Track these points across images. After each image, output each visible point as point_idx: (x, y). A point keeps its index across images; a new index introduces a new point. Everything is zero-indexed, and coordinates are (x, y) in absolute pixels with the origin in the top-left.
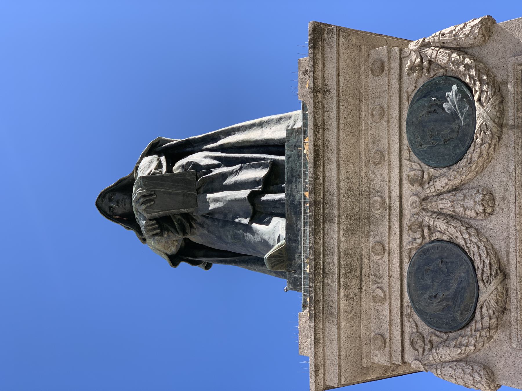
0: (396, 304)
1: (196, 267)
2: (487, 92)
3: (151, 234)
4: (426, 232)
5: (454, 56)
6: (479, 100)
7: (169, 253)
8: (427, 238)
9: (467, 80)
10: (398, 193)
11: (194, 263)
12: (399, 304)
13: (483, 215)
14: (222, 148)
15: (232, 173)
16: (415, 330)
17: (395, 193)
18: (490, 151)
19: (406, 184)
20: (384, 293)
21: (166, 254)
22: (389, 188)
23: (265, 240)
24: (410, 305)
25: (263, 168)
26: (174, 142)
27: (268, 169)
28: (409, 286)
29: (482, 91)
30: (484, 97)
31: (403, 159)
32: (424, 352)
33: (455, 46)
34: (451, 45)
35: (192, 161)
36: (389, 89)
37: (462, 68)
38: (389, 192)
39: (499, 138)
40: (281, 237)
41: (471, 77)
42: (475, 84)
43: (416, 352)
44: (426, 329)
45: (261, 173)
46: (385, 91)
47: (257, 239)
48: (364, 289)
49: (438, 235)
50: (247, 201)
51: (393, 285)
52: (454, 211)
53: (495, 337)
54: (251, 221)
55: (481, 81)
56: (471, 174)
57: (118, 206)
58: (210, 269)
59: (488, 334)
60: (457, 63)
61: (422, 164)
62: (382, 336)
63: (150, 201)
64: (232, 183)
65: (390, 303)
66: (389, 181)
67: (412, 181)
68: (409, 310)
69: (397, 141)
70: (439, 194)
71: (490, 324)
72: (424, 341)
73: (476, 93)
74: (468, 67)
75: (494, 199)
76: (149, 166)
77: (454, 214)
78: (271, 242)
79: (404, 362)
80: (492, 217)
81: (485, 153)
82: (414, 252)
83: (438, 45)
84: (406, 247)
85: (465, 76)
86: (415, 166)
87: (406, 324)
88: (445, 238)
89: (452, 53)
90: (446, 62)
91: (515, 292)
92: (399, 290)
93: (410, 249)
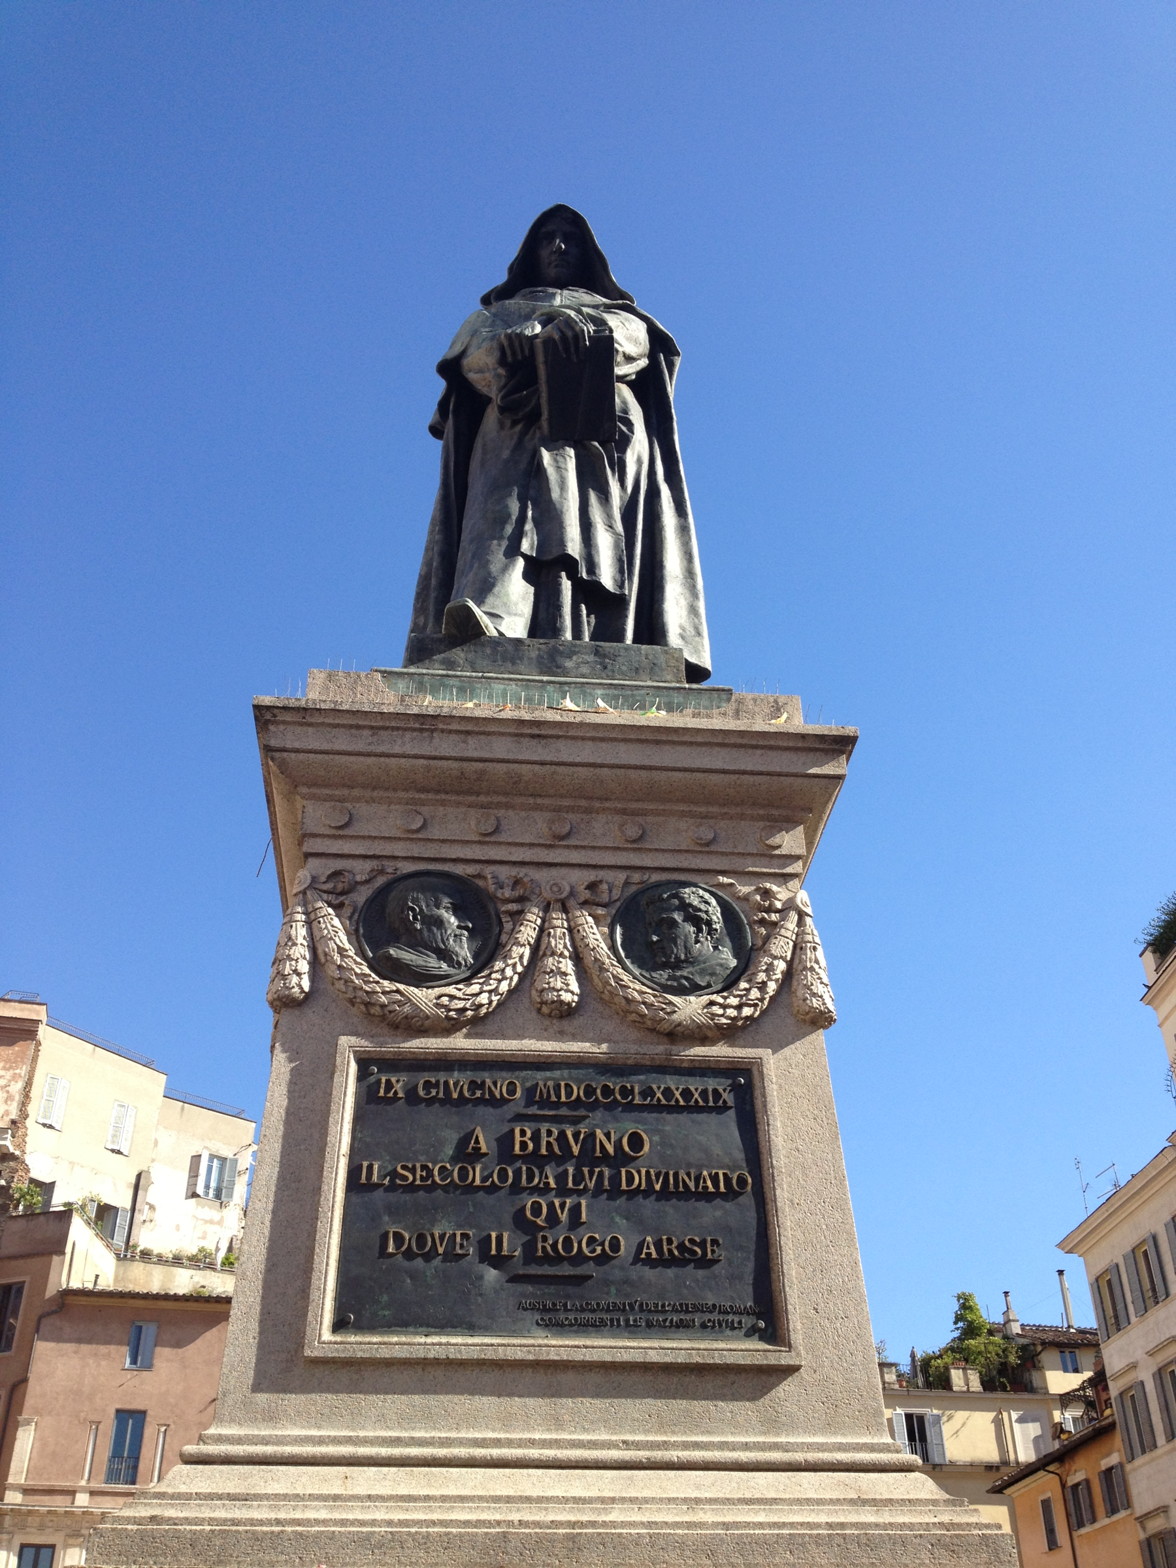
0: (399, 849)
1: (434, 406)
2: (722, 1016)
3: (506, 343)
4: (513, 907)
5: (781, 966)
6: (712, 1003)
7: (466, 362)
8: (503, 909)
9: (743, 985)
10: (574, 861)
11: (443, 406)
12: (400, 854)
13: (539, 1000)
14: (653, 493)
15: (609, 516)
16: (358, 878)
17: (575, 857)
18: (634, 1015)
19: (591, 876)
20: (418, 831)
21: (463, 354)
22: (583, 847)
23: (493, 585)
24: (399, 873)
25: (615, 580)
26: (669, 389)
27: (613, 591)
28: (428, 873)
29: (724, 1007)
30: (717, 1010)
31: (629, 872)
32: (325, 892)
33: (795, 966)
34: (796, 961)
35: (633, 433)
36: (739, 854)
37: (762, 977)
38: (576, 847)
39: (653, 1030)
40: (499, 619)
41: (748, 990)
42: (735, 996)
43: (323, 879)
44: (361, 896)
45: (607, 577)
46: (735, 847)
47: (494, 568)
48: (422, 796)
49: (508, 926)
50: (560, 553)
51: (430, 845)
52: (544, 955)
53: (354, 1010)
54: (525, 556)
55: (739, 1008)
56: (600, 984)
57: (555, 252)
58: (430, 435)
59: (358, 1000)
60: (770, 969)
61: (618, 904)
62: (346, 825)
63: (567, 350)
64: (592, 517)
65: (400, 839)
66: (594, 848)
67: (592, 886)
68: (390, 870)
69: (656, 864)
70: (570, 930)
71: (374, 1005)
72: (342, 893)
73: (722, 997)
74: (763, 987)
75: (561, 1017)
76: (629, 339)
77: (541, 953)
78: (490, 600)
79: (308, 855)
80: (534, 1014)
81: (632, 1008)
82: (481, 883)
83: (799, 940)
84: (488, 871)
85: (749, 981)
86: (616, 894)
87: (369, 865)
88: (504, 938)
89: (786, 962)
90: (773, 952)
91: (423, 1046)
92: (421, 856)
93: (485, 878)
